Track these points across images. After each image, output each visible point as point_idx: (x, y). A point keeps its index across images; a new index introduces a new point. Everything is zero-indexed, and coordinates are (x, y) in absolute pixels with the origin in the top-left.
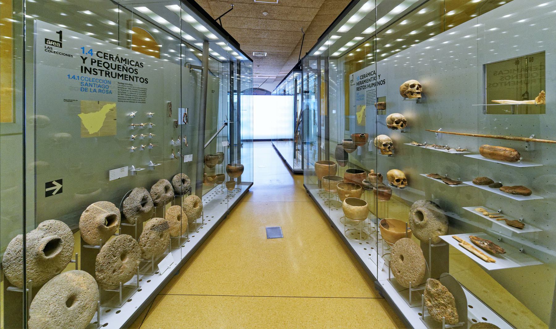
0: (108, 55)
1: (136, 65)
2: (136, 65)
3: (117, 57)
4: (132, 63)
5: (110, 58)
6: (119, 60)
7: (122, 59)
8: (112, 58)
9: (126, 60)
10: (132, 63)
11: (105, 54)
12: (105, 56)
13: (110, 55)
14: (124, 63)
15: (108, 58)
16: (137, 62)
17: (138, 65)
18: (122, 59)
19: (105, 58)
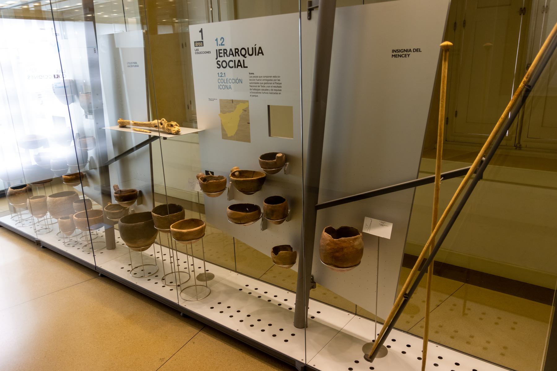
0: (222, 51)
5: (224, 53)
6: (233, 54)
8: (226, 53)
13: (224, 50)
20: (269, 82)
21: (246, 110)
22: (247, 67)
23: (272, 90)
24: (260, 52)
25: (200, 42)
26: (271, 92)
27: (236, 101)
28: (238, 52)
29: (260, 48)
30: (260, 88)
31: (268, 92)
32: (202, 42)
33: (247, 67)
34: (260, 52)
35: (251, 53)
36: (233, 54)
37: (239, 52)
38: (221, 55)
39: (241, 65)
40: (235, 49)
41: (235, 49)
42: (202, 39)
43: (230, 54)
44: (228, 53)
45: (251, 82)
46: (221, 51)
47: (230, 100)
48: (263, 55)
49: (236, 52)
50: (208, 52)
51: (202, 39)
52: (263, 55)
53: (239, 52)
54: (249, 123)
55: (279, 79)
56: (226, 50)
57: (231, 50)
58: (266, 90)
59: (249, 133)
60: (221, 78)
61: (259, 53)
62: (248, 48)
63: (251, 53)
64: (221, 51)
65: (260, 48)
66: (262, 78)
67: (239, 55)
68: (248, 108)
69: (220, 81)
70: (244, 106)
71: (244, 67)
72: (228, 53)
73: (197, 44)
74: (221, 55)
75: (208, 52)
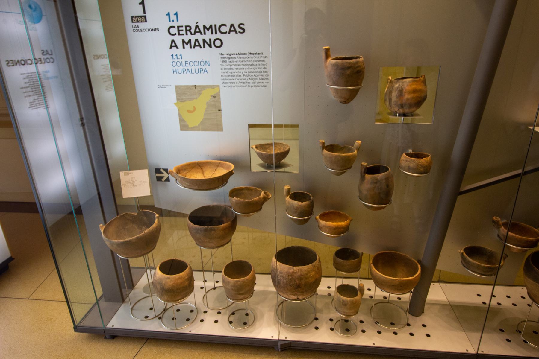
0: (184, 28)
1: (230, 31)
2: (230, 31)
3: (197, 27)
4: (223, 29)
5: (187, 31)
6: (200, 32)
7: (205, 27)
8: (190, 30)
9: (211, 26)
10: (223, 29)
11: (178, 27)
12: (179, 31)
13: (186, 27)
14: (208, 33)
15: (184, 32)
16: (232, 25)
17: (235, 31)
18: (205, 27)
19: (179, 34)
21: (216, 97)
25: (141, 17)
27: (200, 86)
32: (145, 17)
38: (181, 32)
42: (144, 12)
43: (195, 32)
44: (193, 31)
46: (180, 28)
47: (192, 86)
50: (155, 30)
51: (144, 12)
54: (220, 110)
57: (197, 27)
59: (221, 121)
60: (176, 60)
64: (180, 28)
68: (219, 94)
69: (174, 64)
70: (213, 92)
72: (193, 31)
73: (135, 19)
74: (181, 32)
75: (155, 30)
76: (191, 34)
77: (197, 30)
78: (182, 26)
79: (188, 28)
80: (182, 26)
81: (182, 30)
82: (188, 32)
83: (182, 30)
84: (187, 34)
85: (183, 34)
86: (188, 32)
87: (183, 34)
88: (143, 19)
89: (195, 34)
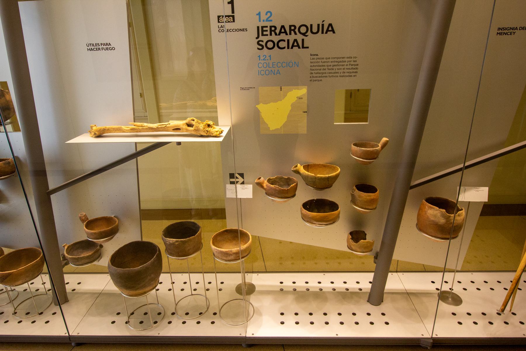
0: (268, 29)
5: (271, 31)
6: (285, 32)
8: (274, 31)
13: (271, 27)
15: (268, 33)
20: (340, 64)
22: (308, 48)
23: (344, 73)
24: (331, 29)
25: (229, 16)
26: (342, 74)
28: (294, 30)
29: (330, 25)
30: (327, 71)
31: (339, 75)
32: (233, 17)
33: (308, 48)
34: (331, 29)
35: (315, 30)
36: (285, 32)
37: (297, 30)
38: (265, 33)
39: (298, 46)
40: (290, 26)
41: (290, 26)
42: (233, 12)
45: (312, 64)
46: (264, 29)
48: (334, 32)
49: (290, 30)
50: (243, 30)
52: (334, 32)
53: (297, 30)
55: (355, 59)
56: (275, 27)
58: (335, 73)
61: (328, 31)
62: (311, 25)
63: (315, 30)
64: (264, 29)
65: (330, 25)
66: (330, 60)
67: (296, 34)
69: (260, 65)
71: (303, 47)
72: (278, 31)
74: (265, 33)
75: (243, 30)
76: (276, 34)
77: (283, 31)
78: (267, 27)
79: (273, 29)
80: (267, 27)
81: (267, 31)
82: (273, 33)
83: (267, 31)
84: (271, 35)
85: (267, 35)
86: (273, 33)
87: (267, 35)
88: (232, 18)
89: (279, 34)
